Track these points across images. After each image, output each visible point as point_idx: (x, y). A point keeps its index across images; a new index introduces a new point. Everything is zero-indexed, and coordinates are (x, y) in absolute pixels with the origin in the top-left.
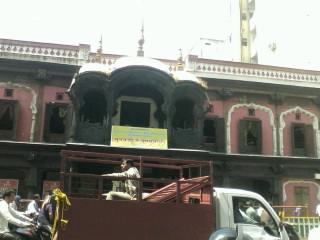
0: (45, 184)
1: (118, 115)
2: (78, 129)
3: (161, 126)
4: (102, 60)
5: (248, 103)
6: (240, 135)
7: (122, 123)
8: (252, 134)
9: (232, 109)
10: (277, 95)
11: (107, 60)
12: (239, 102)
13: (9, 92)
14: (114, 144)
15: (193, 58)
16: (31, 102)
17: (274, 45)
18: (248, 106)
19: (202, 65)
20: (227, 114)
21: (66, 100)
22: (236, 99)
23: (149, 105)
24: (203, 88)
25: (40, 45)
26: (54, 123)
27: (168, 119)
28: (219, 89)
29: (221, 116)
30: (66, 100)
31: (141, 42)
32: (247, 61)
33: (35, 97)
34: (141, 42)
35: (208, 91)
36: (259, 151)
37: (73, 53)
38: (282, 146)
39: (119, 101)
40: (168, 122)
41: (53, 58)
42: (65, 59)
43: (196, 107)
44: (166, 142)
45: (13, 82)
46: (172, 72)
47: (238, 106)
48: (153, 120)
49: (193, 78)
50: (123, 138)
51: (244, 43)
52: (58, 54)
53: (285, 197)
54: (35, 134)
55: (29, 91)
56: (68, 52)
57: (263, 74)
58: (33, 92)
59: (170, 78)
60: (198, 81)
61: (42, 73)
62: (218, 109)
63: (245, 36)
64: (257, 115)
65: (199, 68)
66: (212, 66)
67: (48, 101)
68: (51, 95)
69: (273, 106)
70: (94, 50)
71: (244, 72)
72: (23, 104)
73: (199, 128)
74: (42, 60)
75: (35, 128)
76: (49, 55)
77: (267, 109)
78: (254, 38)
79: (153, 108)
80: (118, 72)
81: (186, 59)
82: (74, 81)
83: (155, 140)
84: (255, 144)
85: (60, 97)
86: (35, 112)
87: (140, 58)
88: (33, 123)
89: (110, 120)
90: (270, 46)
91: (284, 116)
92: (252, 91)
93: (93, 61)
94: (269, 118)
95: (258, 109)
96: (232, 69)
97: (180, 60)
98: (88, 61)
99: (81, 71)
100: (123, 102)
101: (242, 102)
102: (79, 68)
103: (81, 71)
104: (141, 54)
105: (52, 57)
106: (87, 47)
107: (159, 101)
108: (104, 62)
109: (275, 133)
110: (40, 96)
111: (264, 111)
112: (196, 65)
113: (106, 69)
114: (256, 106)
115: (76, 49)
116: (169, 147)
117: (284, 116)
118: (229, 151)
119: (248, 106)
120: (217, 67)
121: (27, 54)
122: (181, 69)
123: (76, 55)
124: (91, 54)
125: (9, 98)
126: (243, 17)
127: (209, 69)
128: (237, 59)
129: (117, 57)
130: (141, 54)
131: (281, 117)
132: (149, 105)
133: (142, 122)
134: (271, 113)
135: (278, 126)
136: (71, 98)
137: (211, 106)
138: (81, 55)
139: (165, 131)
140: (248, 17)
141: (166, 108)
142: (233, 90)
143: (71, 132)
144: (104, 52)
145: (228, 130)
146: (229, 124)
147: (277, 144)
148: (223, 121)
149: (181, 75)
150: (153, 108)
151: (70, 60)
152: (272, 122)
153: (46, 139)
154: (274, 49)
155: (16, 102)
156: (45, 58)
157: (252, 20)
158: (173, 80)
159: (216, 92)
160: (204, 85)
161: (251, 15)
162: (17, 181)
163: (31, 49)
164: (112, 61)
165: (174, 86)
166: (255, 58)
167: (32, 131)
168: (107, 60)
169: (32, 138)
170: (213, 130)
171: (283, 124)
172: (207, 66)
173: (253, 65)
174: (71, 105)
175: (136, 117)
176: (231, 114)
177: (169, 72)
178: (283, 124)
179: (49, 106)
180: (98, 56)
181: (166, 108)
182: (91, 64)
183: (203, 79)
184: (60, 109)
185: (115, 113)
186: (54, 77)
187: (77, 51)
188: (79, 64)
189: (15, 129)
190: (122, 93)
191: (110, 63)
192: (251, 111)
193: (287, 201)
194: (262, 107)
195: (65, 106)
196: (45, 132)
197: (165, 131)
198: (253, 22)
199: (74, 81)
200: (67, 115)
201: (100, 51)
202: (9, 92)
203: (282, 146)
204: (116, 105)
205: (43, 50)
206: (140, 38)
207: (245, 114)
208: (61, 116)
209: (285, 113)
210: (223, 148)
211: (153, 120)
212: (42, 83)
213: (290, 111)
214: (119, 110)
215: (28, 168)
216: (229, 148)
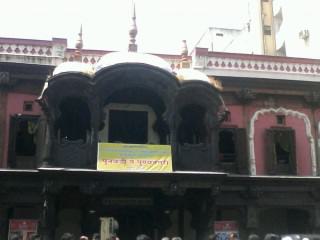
1: (106, 129)
2: (53, 149)
3: (163, 142)
4: (83, 58)
5: (276, 107)
6: (267, 150)
7: (112, 139)
8: (283, 147)
9: (255, 116)
11: (89, 58)
12: (264, 107)
15: (201, 52)
17: (306, 32)
18: (276, 111)
19: (213, 60)
20: (249, 123)
21: (37, 110)
23: (144, 115)
24: (216, 90)
25: (34, 43)
27: (172, 131)
28: (237, 90)
29: (240, 126)
30: (37, 110)
31: (133, 33)
32: (271, 53)
34: (133, 33)
35: (223, 93)
37: (45, 50)
39: (107, 111)
40: (172, 136)
41: (18, 57)
42: (34, 58)
43: (207, 115)
44: (169, 159)
46: (176, 70)
47: (263, 111)
48: (151, 134)
49: (203, 77)
50: (115, 160)
51: (267, 31)
52: (25, 51)
57: (294, 69)
59: (172, 78)
62: (236, 118)
63: (268, 23)
64: (288, 124)
65: (210, 64)
66: (227, 61)
67: (13, 114)
69: (309, 111)
70: (71, 45)
71: (269, 68)
73: (214, 139)
76: (13, 53)
77: (301, 114)
78: (279, 25)
79: (152, 119)
80: (104, 73)
81: (191, 51)
82: (46, 85)
83: (154, 160)
84: (287, 162)
85: (28, 107)
89: (95, 137)
90: (301, 34)
92: (280, 92)
93: (71, 60)
94: (304, 125)
95: (290, 115)
96: (253, 64)
98: (65, 60)
99: (56, 72)
100: (111, 111)
101: (268, 107)
103: (56, 72)
104: (133, 48)
106: (63, 41)
107: (159, 108)
108: (86, 61)
109: (313, 146)
112: (206, 60)
113: (88, 68)
114: (287, 112)
115: (48, 44)
116: (174, 169)
119: (276, 111)
120: (233, 62)
122: (186, 66)
123: (49, 53)
124: (69, 50)
127: (223, 65)
128: (259, 52)
130: (133, 48)
132: (144, 115)
133: (140, 138)
136: (44, 108)
137: (228, 113)
139: (168, 148)
141: (169, 117)
142: (254, 91)
143: (44, 153)
145: (252, 144)
146: (251, 135)
148: (244, 132)
149: (187, 74)
150: (152, 119)
151: (40, 59)
152: (309, 131)
153: (11, 164)
154: (306, 38)
158: (176, 80)
159: (233, 93)
160: (217, 85)
164: (96, 59)
165: (178, 88)
166: (283, 50)
168: (89, 58)
170: (231, 145)
172: (220, 61)
173: (281, 58)
174: (43, 116)
175: (130, 132)
176: (255, 123)
177: (171, 70)
179: (14, 119)
180: (78, 53)
181: (169, 117)
182: (68, 63)
184: (29, 123)
185: (101, 127)
186: (21, 81)
188: (53, 64)
190: (107, 103)
191: (93, 61)
192: (281, 118)
194: (294, 112)
195: (36, 119)
196: (9, 153)
197: (168, 148)
199: (46, 85)
200: (37, 131)
201: (79, 46)
204: (102, 116)
206: (132, 28)
207: (273, 122)
208: (30, 132)
210: (246, 168)
211: (151, 134)
214: (106, 122)
216: (253, 167)
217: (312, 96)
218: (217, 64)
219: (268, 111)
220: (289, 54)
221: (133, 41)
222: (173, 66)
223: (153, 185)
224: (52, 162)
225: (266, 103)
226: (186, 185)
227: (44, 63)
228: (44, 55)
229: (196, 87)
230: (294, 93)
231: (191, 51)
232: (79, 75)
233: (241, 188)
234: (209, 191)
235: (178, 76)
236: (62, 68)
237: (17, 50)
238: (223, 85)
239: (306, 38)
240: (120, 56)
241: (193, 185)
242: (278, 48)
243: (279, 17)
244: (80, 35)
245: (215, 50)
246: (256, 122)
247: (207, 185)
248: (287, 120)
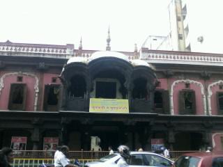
0: (45, 139)
1: (95, 91)
3: (124, 98)
5: (185, 79)
6: (180, 102)
8: (188, 99)
9: (174, 84)
10: (206, 73)
11: (86, 54)
12: (178, 79)
13: (20, 79)
14: (91, 111)
15: (145, 50)
16: (35, 84)
17: (202, 38)
18: (185, 81)
19: (151, 54)
21: (59, 82)
22: (176, 77)
23: (115, 84)
24: (153, 70)
26: (50, 96)
27: (129, 92)
28: (164, 70)
29: (166, 89)
30: (59, 82)
31: (109, 41)
32: (183, 50)
33: (38, 81)
34: (109, 41)
35: (156, 72)
36: (194, 112)
37: (63, 50)
38: (210, 108)
39: (95, 83)
40: (129, 95)
42: (57, 55)
43: (148, 84)
45: (23, 72)
46: (131, 60)
47: (178, 81)
48: (118, 94)
49: (145, 63)
50: (99, 106)
51: (180, 37)
53: (214, 144)
54: (37, 106)
55: (33, 77)
56: (59, 50)
57: (195, 59)
58: (36, 78)
59: (129, 64)
60: (148, 65)
61: (42, 65)
62: (164, 84)
63: (181, 32)
64: (192, 88)
65: (149, 56)
68: (48, 80)
69: (203, 81)
70: (76, 48)
72: (29, 86)
73: (151, 98)
74: (42, 56)
75: (37, 103)
78: (187, 34)
80: (93, 62)
81: (139, 49)
82: (64, 69)
83: (119, 106)
84: (191, 108)
85: (54, 80)
86: (37, 91)
87: (108, 52)
88: (36, 98)
89: (89, 95)
90: (198, 39)
91: (211, 87)
93: (76, 56)
94: (200, 88)
97: (136, 51)
98: (73, 56)
99: (69, 62)
100: (97, 83)
102: (67, 60)
103: (69, 62)
104: (108, 49)
105: (49, 54)
106: (71, 46)
107: (122, 80)
108: (84, 56)
109: (205, 99)
110: (41, 81)
111: (197, 85)
112: (146, 55)
114: (191, 81)
115: (64, 48)
116: (131, 110)
117: (211, 87)
118: (173, 114)
119: (185, 81)
121: (32, 52)
122: (137, 58)
123: (65, 52)
124: (75, 51)
125: (20, 83)
126: (179, 19)
127: (157, 57)
128: (176, 49)
129: (92, 52)
130: (108, 49)
131: (209, 89)
133: (113, 96)
134: (202, 86)
135: (207, 95)
136: (62, 81)
137: (159, 83)
138: (68, 51)
139: (127, 101)
140: (182, 18)
141: (127, 85)
142: (174, 71)
143: (60, 103)
144: (83, 49)
145: (172, 98)
146: (172, 94)
147: (207, 106)
148: (167, 92)
149: (138, 62)
150: (118, 86)
151: (60, 55)
152: (203, 92)
153: (45, 110)
154: (201, 41)
155: (25, 85)
156: (44, 54)
157: (185, 21)
160: (153, 68)
161: (184, 17)
162: (26, 138)
163: (34, 49)
164: (89, 55)
165: (132, 70)
166: (189, 48)
167: (36, 104)
169: (35, 108)
170: (161, 99)
171: (210, 93)
172: (155, 55)
173: (187, 52)
174: (62, 85)
175: (107, 92)
176: (173, 88)
177: (128, 60)
178: (210, 93)
179: (47, 87)
180: (80, 52)
181: (127, 85)
183: (153, 64)
185: (92, 90)
186: (51, 67)
187: (65, 49)
188: (67, 58)
189: (24, 102)
190: (94, 78)
191: (88, 56)
192: (187, 85)
193: (215, 147)
194: (195, 82)
195: (58, 86)
196: (44, 104)
198: (186, 23)
199: (64, 69)
200: (59, 92)
201: (80, 48)
202: (20, 79)
203: (210, 108)
204: (92, 85)
205: (43, 49)
207: (183, 87)
208: (55, 93)
209: (212, 85)
210: (169, 112)
211: (118, 94)
212: (42, 71)
213: (215, 83)
214: (95, 88)
215: (33, 129)
216: (172, 111)
217: (204, 73)
218: (153, 57)
219: (181, 81)
220: (193, 50)
221: (108, 45)
222: (129, 58)
223: (119, 120)
224: (65, 107)
225: (180, 77)
226: (136, 120)
227: (64, 58)
228: (62, 53)
229: (142, 69)
230: (194, 71)
231: (139, 49)
232: (80, 63)
233: (166, 122)
234: (148, 123)
235: (132, 63)
236: (72, 60)
237: (48, 51)
238: (156, 68)
239: (201, 41)
240: (102, 53)
241: (140, 120)
242: (187, 46)
243: (187, 29)
244: (81, 42)
245: (153, 49)
246: (174, 87)
247: (148, 120)
248: (191, 86)
